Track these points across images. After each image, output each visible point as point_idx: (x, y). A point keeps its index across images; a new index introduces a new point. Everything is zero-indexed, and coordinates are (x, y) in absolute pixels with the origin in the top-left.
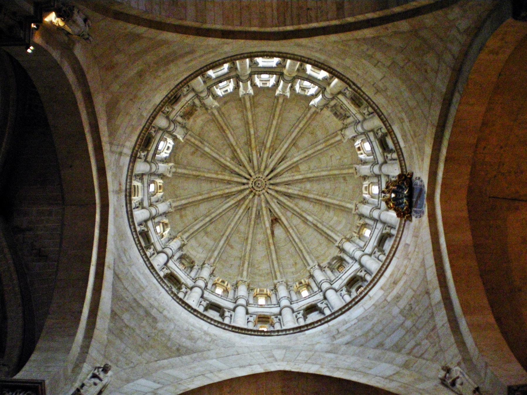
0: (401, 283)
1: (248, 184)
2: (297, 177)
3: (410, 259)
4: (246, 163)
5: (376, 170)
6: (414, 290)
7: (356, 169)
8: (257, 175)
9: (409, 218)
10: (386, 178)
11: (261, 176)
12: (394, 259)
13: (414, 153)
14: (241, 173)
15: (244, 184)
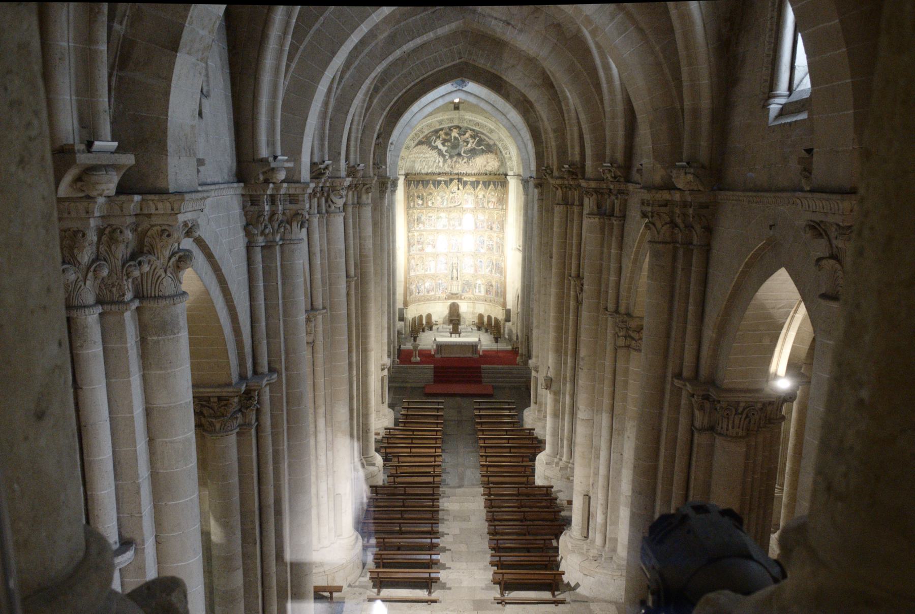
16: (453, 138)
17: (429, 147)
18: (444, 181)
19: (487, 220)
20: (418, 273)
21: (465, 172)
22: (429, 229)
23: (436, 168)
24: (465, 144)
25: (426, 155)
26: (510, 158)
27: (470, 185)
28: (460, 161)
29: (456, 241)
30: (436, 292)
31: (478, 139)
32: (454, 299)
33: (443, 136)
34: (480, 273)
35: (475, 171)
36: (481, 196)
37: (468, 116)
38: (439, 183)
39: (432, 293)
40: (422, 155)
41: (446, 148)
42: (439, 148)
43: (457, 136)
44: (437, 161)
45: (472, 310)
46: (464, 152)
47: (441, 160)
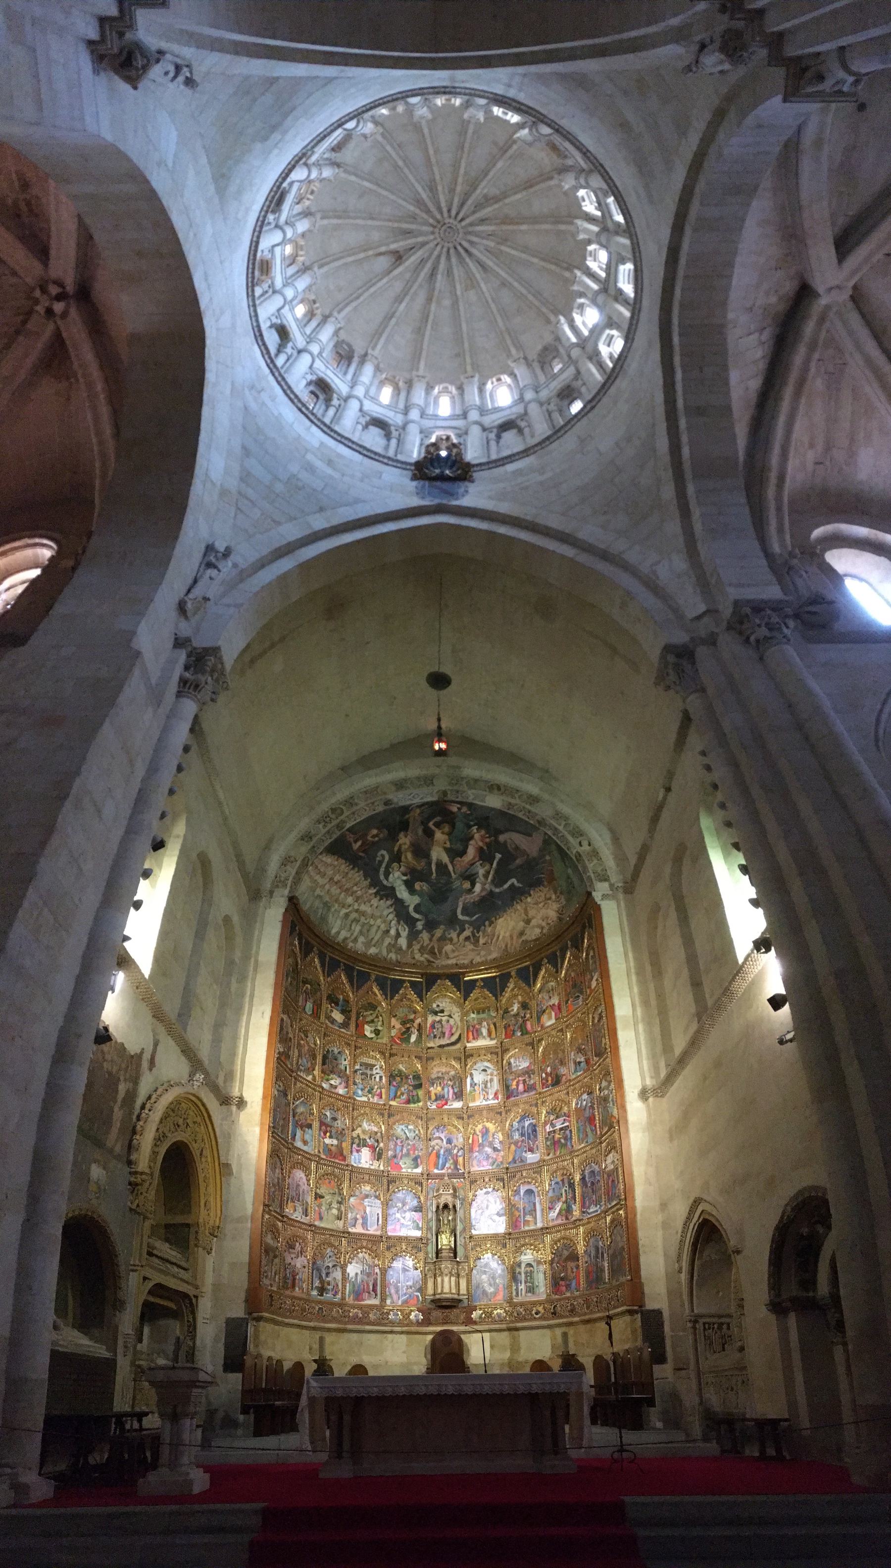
0: (330, 471)
1: (450, 217)
2: (458, 287)
3: (362, 481)
4: (478, 215)
5: (474, 415)
6: (323, 489)
7: (472, 377)
8: (461, 231)
9: (414, 478)
10: (464, 428)
11: (461, 235)
12: (361, 457)
13: (501, 485)
14: (465, 208)
15: (449, 211)
17: (372, 885)
18: (410, 981)
21: (466, 962)
23: (389, 951)
24: (467, 885)
25: (363, 908)
27: (482, 987)
28: (454, 935)
31: (498, 856)
33: (409, 855)
35: (494, 955)
36: (516, 1008)
37: (471, 770)
38: (397, 986)
41: (416, 900)
42: (399, 896)
43: (445, 859)
44: (393, 932)
45: (507, 1355)
46: (465, 911)
47: (404, 933)
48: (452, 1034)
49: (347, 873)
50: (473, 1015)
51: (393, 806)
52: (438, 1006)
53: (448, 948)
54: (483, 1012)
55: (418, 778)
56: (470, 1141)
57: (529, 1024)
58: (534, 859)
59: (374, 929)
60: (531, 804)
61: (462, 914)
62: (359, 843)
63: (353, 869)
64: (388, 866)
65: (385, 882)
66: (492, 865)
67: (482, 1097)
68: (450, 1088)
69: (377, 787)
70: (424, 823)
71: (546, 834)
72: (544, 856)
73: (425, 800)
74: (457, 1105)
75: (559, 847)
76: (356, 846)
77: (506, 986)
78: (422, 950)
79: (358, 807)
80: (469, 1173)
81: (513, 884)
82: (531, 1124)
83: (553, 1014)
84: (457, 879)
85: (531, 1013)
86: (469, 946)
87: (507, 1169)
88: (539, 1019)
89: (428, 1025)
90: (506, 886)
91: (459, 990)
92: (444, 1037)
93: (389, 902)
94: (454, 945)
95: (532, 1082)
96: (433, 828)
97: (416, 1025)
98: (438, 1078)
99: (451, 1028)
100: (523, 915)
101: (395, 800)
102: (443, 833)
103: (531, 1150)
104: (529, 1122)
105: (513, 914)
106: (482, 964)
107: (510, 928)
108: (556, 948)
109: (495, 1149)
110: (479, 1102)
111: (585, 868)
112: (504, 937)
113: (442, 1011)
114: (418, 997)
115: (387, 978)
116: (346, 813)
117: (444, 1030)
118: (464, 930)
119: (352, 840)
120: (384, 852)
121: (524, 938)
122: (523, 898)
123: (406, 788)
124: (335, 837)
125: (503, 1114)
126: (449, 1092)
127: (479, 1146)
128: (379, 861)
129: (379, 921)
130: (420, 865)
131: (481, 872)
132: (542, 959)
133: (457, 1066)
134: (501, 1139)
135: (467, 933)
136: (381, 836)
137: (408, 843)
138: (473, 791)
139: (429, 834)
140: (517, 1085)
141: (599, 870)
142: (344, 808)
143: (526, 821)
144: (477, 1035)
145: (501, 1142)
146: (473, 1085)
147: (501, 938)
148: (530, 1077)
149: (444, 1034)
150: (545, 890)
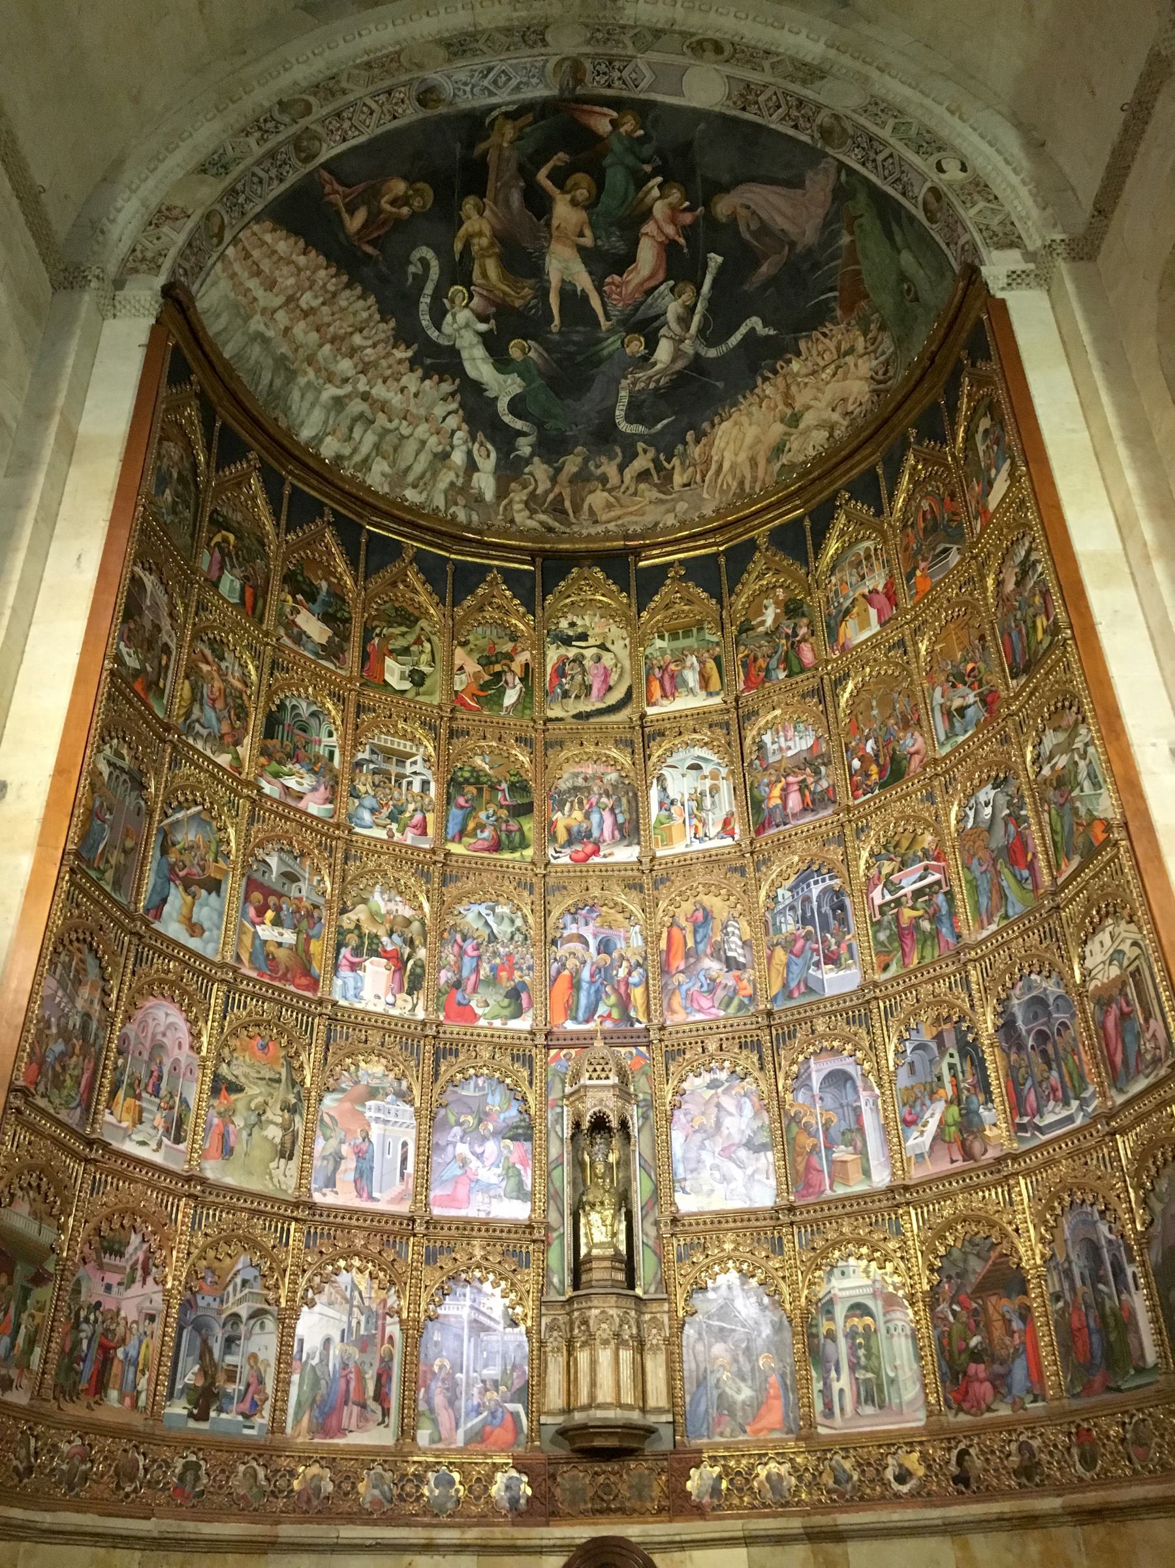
16: (554, 301)
18: (501, 570)
19: (855, 728)
20: (212, 1170)
22: (382, 834)
24: (637, 346)
26: (980, 187)
27: (682, 578)
29: (605, 947)
30: (406, 1432)
31: (715, 260)
32: (603, 1510)
34: (858, 1187)
36: (770, 616)
39: (382, 1437)
40: (345, 366)
42: (471, 372)
43: (583, 280)
44: (458, 457)
47: (487, 463)
48: (610, 688)
49: (334, 295)
50: (659, 643)
51: (442, 110)
52: (572, 625)
53: (597, 499)
54: (687, 633)
55: (508, 31)
56: (663, 945)
57: (807, 655)
58: (809, 251)
59: (411, 447)
60: (804, 82)
61: (628, 419)
62: (361, 216)
63: (349, 286)
64: (439, 294)
65: (433, 334)
66: (699, 288)
67: (690, 833)
68: (607, 815)
69: (398, 53)
70: (526, 172)
71: (841, 165)
72: (835, 235)
73: (528, 94)
74: (626, 854)
75: (878, 197)
76: (355, 222)
77: (744, 570)
78: (533, 503)
79: (351, 97)
80: (662, 1028)
81: (753, 329)
82: (824, 891)
83: (873, 613)
84: (612, 331)
85: (810, 625)
86: (649, 492)
87: (770, 1014)
88: (832, 633)
89: (549, 669)
90: (734, 340)
91: (625, 588)
92: (588, 694)
93: (447, 387)
94: (610, 491)
95: (824, 784)
96: (548, 184)
97: (516, 666)
98: (576, 789)
99: (607, 674)
100: (781, 407)
101: (449, 89)
102: (574, 203)
103: (832, 959)
104: (821, 886)
105: (754, 409)
106: (683, 525)
107: (749, 440)
108: (872, 459)
109: (731, 964)
110: (682, 845)
111: (954, 225)
112: (733, 467)
113: (583, 637)
114: (522, 604)
115: (448, 559)
116: (319, 111)
117: (589, 679)
118: (636, 455)
119: (337, 199)
120: (427, 252)
121: (784, 459)
122: (780, 363)
123: (475, 53)
124: (292, 179)
125: (750, 869)
126: (604, 824)
127: (687, 955)
128: (415, 275)
129: (422, 430)
130: (521, 296)
131: (673, 309)
132: (835, 496)
133: (625, 759)
134: (746, 937)
135: (641, 463)
136: (417, 203)
137: (487, 230)
138: (654, 57)
139: (539, 205)
140: (784, 798)
141: (994, 223)
142: (311, 99)
143: (791, 139)
144: (673, 685)
145: (745, 943)
146: (667, 804)
147: (726, 466)
148: (817, 772)
149: (589, 688)
150: (837, 331)
